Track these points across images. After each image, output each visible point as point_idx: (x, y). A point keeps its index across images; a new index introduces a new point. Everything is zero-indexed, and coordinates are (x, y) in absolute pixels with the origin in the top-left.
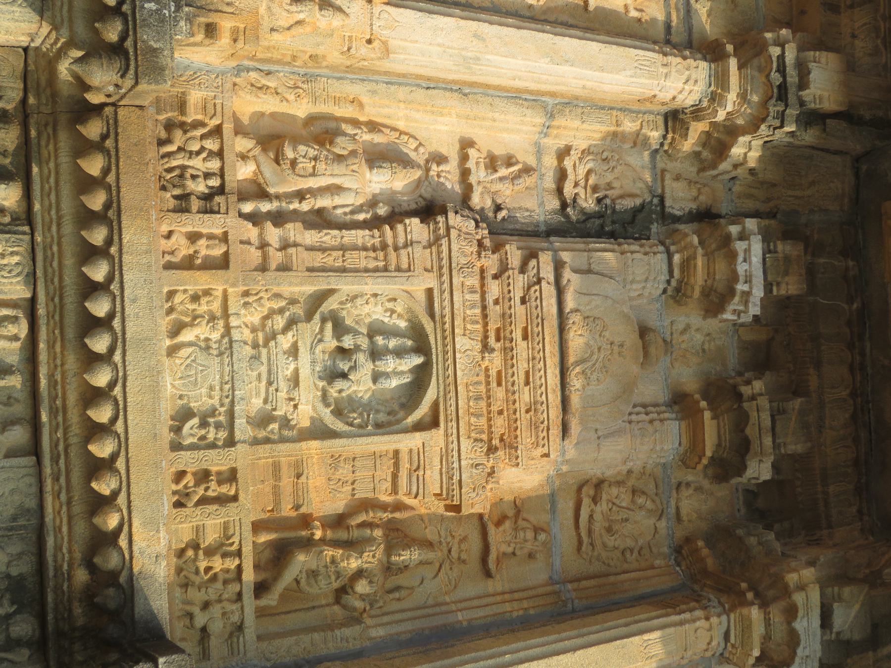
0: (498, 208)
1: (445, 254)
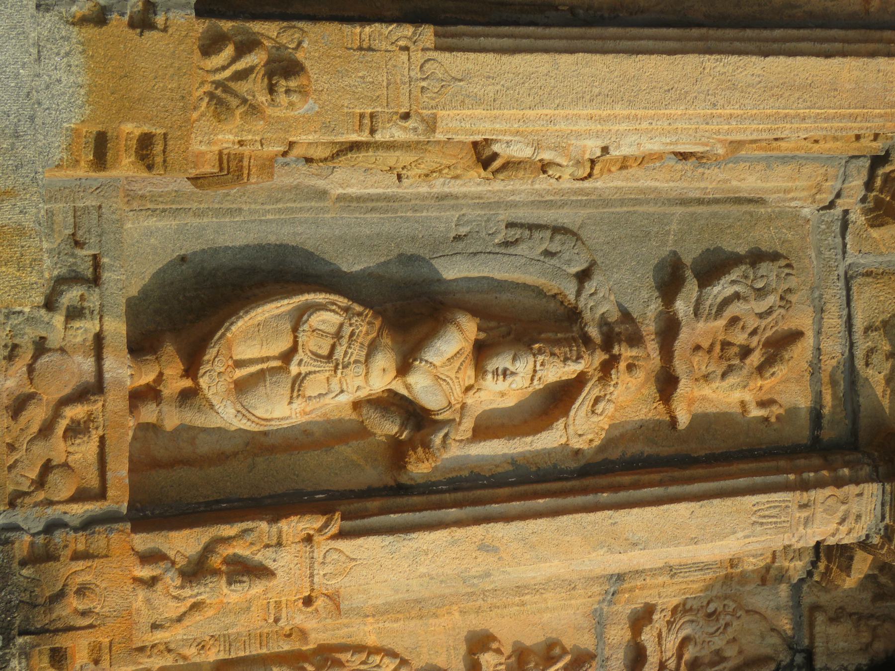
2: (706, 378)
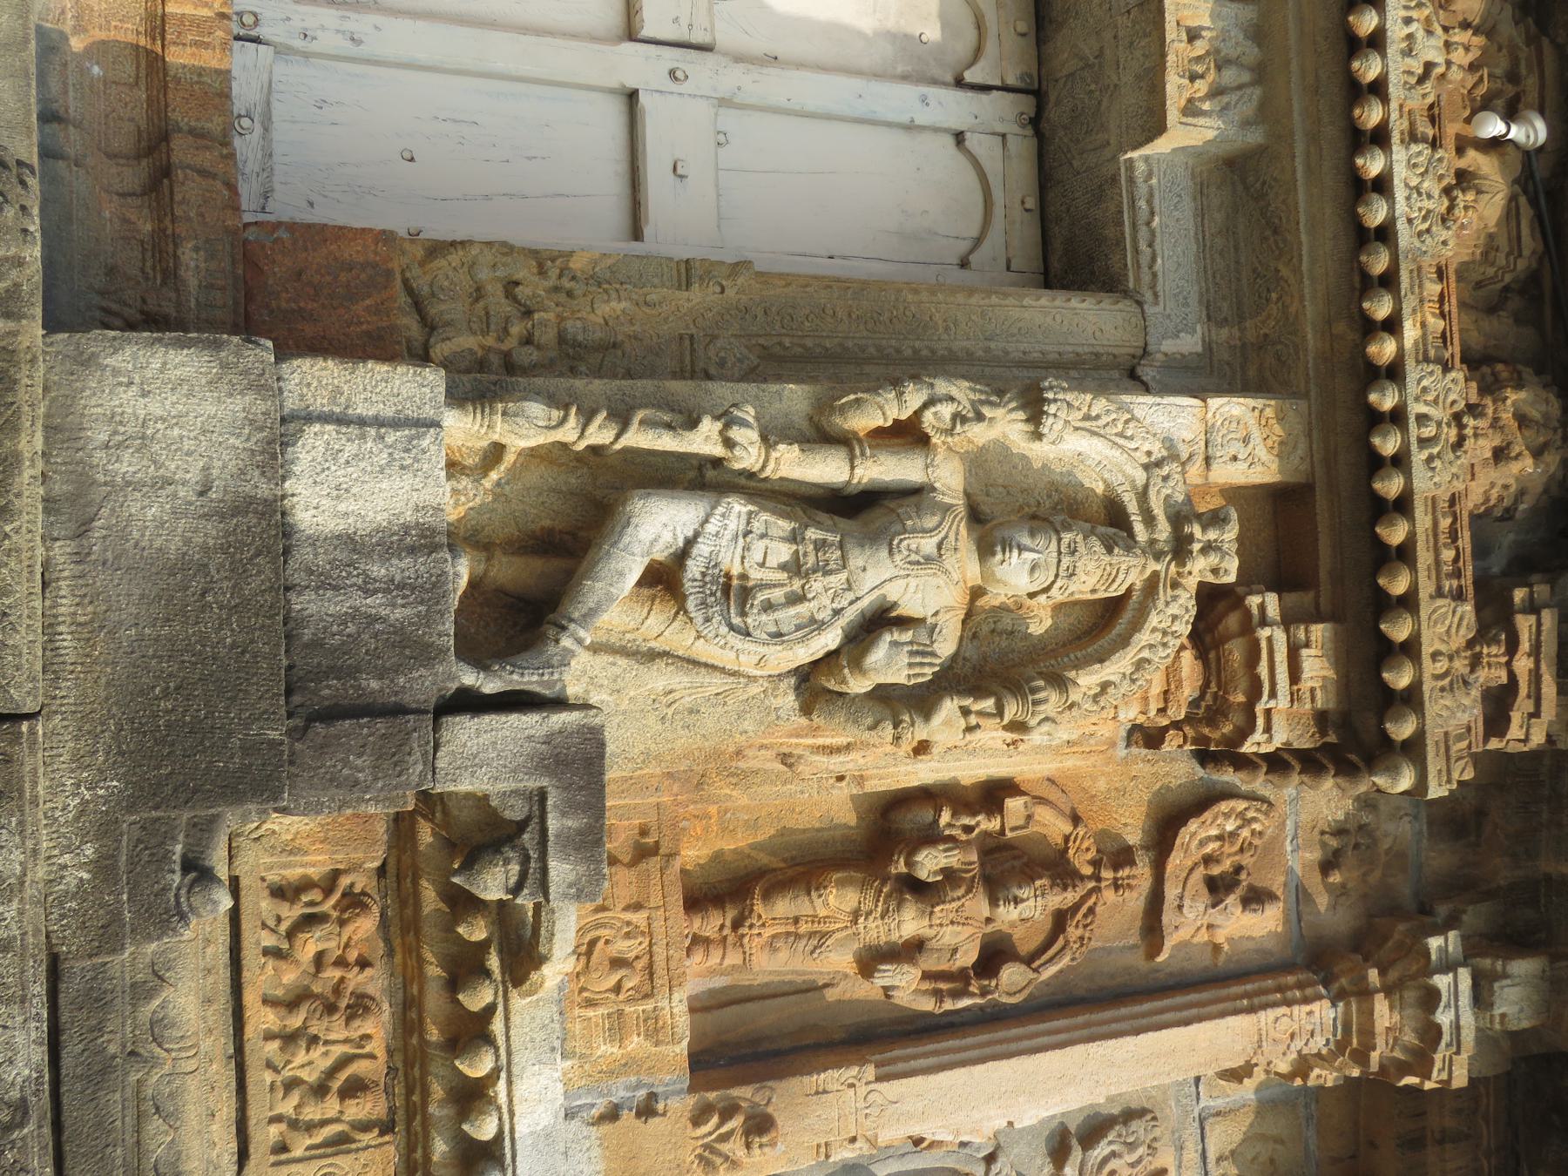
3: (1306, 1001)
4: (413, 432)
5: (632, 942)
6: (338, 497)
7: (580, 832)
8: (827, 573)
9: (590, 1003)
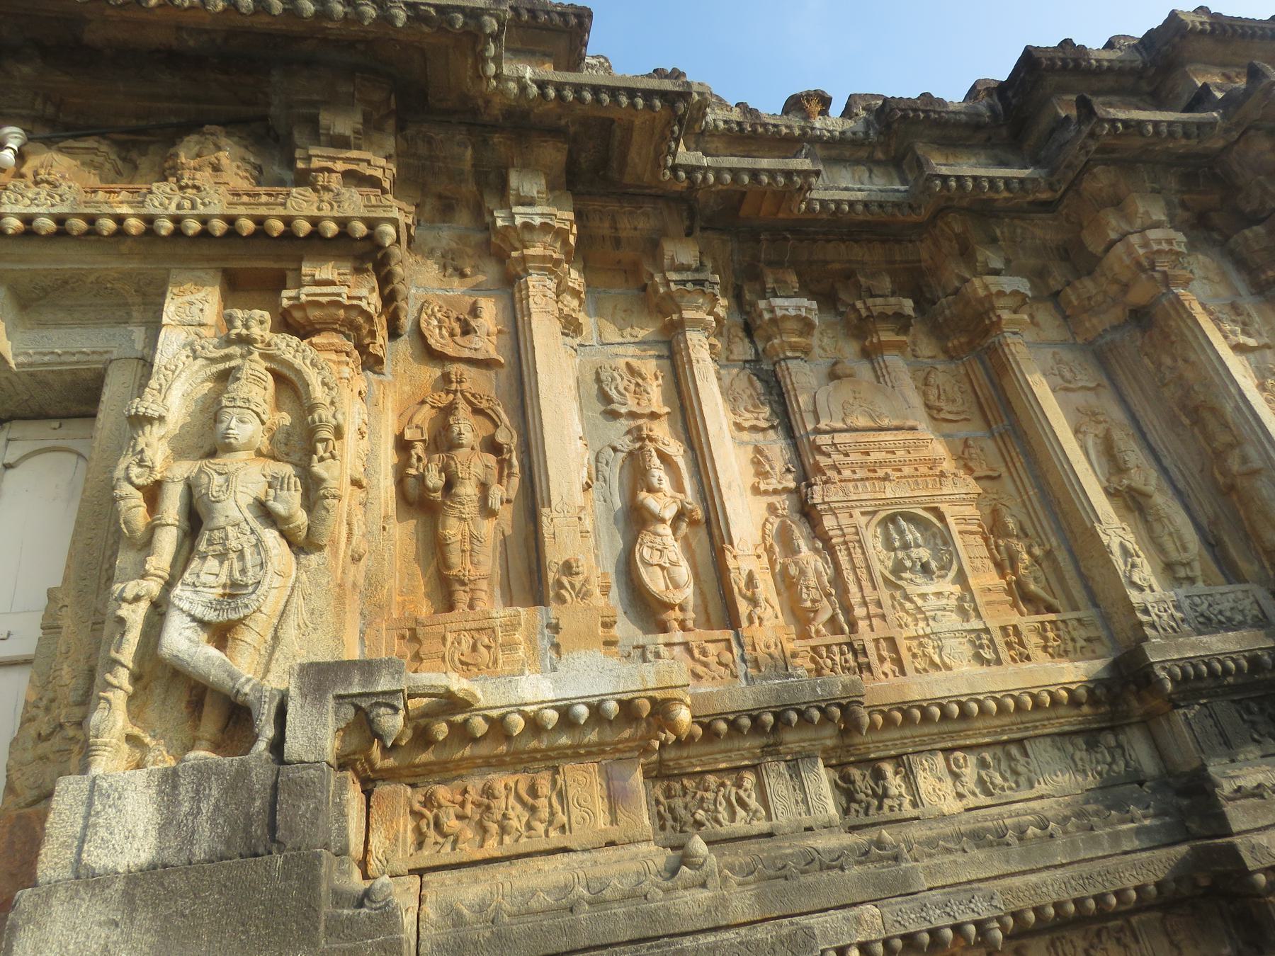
0: (788, 470)
1: (840, 505)
2: (649, 400)
3: (527, 288)
4: (96, 793)
5: (463, 641)
6: (134, 837)
7: (362, 674)
8: (227, 538)
9: (495, 662)
